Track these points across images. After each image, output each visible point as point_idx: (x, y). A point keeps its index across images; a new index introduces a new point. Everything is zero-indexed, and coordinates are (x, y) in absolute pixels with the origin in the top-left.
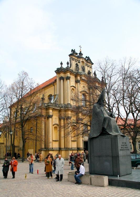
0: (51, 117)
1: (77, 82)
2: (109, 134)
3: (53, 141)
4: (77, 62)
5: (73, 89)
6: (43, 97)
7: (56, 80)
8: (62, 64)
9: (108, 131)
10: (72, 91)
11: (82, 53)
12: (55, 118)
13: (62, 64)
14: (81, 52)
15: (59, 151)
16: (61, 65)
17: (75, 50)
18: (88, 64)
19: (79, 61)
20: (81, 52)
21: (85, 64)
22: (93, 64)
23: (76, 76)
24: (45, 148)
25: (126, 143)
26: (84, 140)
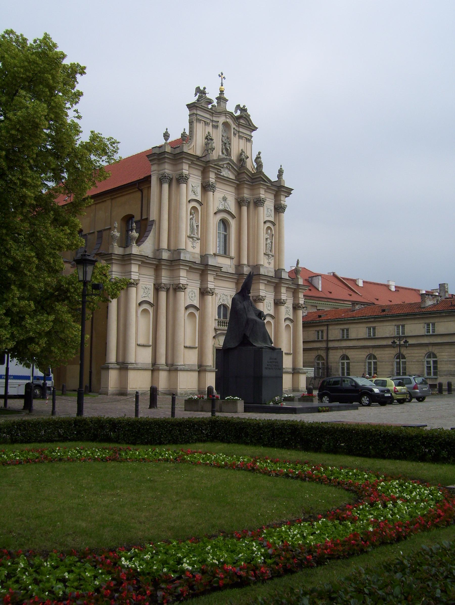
0: (135, 284)
2: (252, 345)
3: (139, 345)
4: (211, 124)
5: (194, 208)
7: (150, 177)
9: (251, 340)
11: (226, 96)
12: (144, 286)
13: (166, 136)
14: (222, 92)
15: (153, 371)
17: (205, 88)
18: (241, 130)
20: (222, 92)
23: (204, 173)
24: (117, 363)
25: (276, 359)
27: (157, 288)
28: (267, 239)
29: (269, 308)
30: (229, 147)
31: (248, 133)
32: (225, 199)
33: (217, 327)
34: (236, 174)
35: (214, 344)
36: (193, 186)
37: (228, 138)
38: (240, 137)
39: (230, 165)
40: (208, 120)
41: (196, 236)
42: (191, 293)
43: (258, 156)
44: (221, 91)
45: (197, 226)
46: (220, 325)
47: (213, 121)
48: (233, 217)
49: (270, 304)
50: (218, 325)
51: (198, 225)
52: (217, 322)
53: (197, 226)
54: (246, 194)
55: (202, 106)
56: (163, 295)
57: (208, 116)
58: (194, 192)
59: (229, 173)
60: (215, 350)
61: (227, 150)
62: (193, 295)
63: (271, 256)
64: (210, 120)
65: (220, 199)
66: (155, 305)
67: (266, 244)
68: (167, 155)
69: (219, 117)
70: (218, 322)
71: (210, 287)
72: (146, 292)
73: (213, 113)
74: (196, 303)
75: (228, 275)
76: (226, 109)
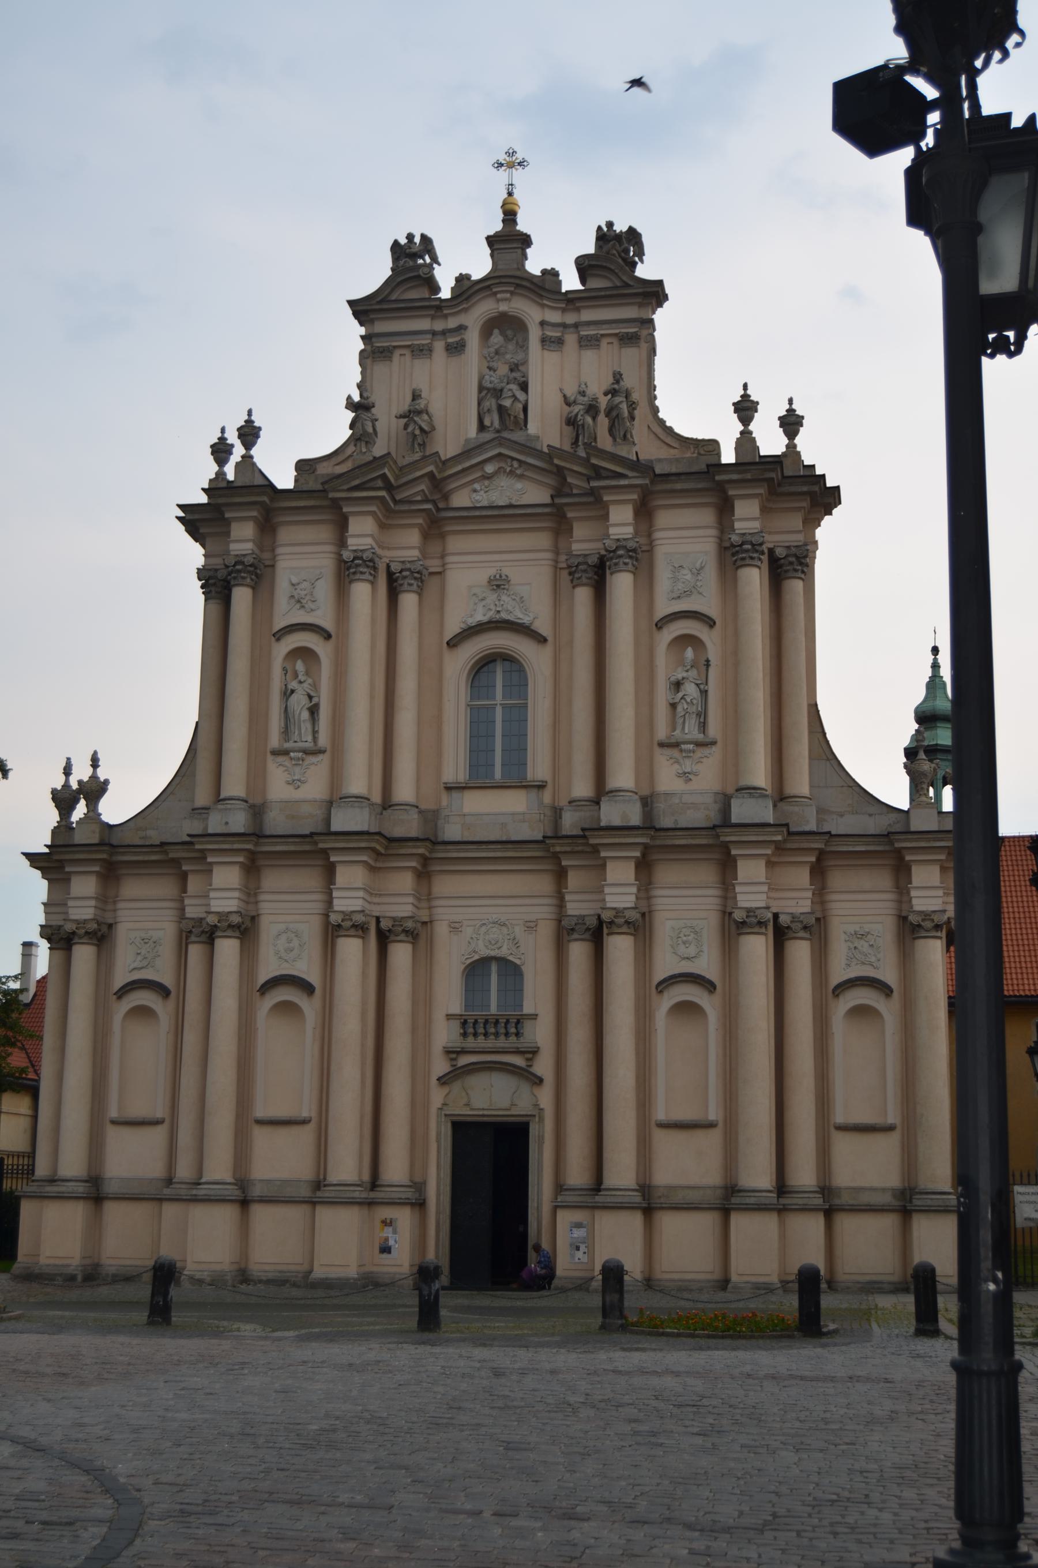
4: (439, 346)
11: (522, 226)
13: (220, 451)
14: (510, 215)
20: (510, 215)
26: (460, 1110)
29: (692, 951)
30: (515, 398)
31: (630, 312)
34: (551, 481)
35: (445, 1104)
36: (295, 580)
37: (514, 368)
38: (589, 343)
39: (513, 459)
40: (424, 336)
41: (309, 745)
42: (284, 937)
43: (616, 386)
45: (314, 711)
46: (475, 1035)
47: (444, 333)
48: (542, 640)
49: (696, 933)
50: (465, 1035)
52: (456, 1025)
53: (314, 711)
55: (396, 301)
56: (195, 952)
57: (424, 324)
58: (299, 601)
59: (519, 485)
60: (447, 1130)
61: (501, 409)
62: (295, 943)
63: (691, 746)
64: (434, 333)
67: (673, 706)
70: (464, 1023)
71: (344, 909)
72: (143, 952)
74: (308, 968)
75: (494, 850)
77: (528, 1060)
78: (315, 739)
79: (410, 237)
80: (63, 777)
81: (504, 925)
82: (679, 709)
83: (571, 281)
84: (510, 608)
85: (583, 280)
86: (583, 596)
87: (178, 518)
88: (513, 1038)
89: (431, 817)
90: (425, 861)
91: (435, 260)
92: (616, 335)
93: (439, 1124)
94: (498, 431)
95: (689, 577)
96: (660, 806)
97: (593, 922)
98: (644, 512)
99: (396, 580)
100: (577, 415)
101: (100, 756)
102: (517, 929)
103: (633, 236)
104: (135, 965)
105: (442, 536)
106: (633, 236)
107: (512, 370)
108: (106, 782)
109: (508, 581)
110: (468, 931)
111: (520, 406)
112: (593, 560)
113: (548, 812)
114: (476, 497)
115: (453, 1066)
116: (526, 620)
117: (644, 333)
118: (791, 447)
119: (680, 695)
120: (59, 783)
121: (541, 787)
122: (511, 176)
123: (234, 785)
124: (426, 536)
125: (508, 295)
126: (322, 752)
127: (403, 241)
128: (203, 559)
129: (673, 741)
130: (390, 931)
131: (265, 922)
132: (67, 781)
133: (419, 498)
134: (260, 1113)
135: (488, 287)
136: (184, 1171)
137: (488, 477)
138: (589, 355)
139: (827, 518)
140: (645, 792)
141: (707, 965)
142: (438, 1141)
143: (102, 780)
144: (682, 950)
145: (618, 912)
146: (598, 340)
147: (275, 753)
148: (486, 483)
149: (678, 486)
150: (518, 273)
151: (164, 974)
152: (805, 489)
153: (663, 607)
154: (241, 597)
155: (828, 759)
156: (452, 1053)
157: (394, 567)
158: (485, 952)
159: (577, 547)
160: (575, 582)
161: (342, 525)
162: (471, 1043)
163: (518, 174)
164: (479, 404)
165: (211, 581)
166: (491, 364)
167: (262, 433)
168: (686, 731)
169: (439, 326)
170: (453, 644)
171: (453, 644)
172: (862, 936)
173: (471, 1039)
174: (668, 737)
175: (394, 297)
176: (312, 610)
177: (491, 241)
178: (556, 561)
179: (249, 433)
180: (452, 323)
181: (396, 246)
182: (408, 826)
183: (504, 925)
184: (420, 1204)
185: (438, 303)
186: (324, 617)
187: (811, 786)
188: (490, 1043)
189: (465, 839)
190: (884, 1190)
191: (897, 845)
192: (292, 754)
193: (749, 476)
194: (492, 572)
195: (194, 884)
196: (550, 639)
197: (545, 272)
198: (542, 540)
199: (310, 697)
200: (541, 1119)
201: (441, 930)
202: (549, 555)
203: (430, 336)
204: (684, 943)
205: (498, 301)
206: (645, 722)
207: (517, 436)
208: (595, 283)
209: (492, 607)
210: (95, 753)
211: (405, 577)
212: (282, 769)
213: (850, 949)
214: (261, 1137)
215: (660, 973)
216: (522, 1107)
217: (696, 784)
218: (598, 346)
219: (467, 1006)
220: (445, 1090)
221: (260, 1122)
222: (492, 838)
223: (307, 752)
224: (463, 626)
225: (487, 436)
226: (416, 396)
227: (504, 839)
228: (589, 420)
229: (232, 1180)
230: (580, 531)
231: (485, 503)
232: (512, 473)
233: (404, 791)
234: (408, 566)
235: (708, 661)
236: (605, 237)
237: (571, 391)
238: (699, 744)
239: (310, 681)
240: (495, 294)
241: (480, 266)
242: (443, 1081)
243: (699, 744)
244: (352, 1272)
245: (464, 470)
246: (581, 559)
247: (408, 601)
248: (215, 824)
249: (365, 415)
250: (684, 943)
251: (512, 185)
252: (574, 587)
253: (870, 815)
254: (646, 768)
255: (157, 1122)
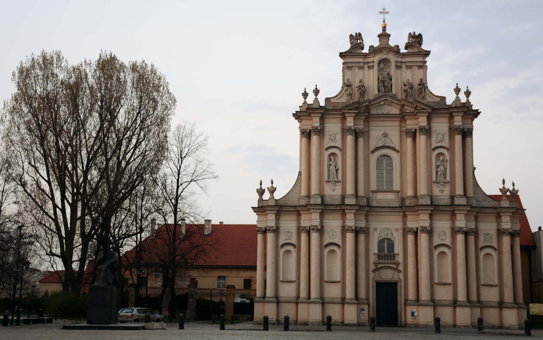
1: (345, 131)
6: (261, 188)
8: (305, 95)
10: (330, 160)
11: (388, 31)
13: (305, 95)
14: (384, 28)
16: (305, 98)
19: (371, 64)
20: (384, 28)
21: (393, 65)
22: (427, 53)
26: (379, 280)
27: (300, 230)
28: (438, 167)
29: (444, 238)
30: (388, 83)
31: (420, 59)
32: (385, 135)
33: (377, 261)
34: (399, 107)
35: (374, 277)
36: (330, 134)
38: (408, 67)
39: (389, 100)
41: (336, 180)
42: (331, 232)
44: (383, 28)
45: (337, 170)
46: (382, 259)
48: (398, 151)
49: (445, 233)
50: (379, 259)
51: (338, 169)
52: (376, 257)
54: (411, 124)
55: (353, 53)
56: (304, 236)
57: (361, 60)
58: (332, 140)
59: (390, 108)
60: (375, 284)
63: (443, 183)
64: (364, 63)
65: (378, 137)
66: (297, 246)
67: (437, 172)
68: (300, 113)
69: (374, 57)
70: (379, 256)
72: (288, 235)
73: (366, 56)
74: (338, 240)
75: (387, 209)
76: (388, 44)
77: (397, 266)
78: (337, 178)
79: (356, 34)
80: (260, 186)
81: (389, 229)
82: (439, 173)
83: (403, 50)
84: (388, 142)
85: (406, 48)
86: (409, 140)
87: (293, 114)
88: (392, 260)
89: (368, 199)
90: (368, 211)
91: (362, 40)
92: (417, 65)
93: (372, 282)
94: (384, 93)
95: (441, 137)
96: (434, 199)
97: (415, 230)
98: (429, 119)
99: (357, 134)
100: (407, 89)
101: (273, 180)
102: (393, 230)
103: (420, 36)
104: (286, 238)
105: (368, 121)
106: (420, 36)
107: (387, 75)
108: (276, 188)
109: (388, 135)
110: (379, 231)
111: (390, 85)
112: (413, 130)
113: (400, 199)
114: (378, 111)
115: (376, 267)
116: (393, 146)
117: (424, 65)
118: (468, 100)
119: (439, 169)
120: (259, 187)
121: (398, 192)
122: (384, 16)
123: (314, 191)
124: (364, 121)
125: (386, 53)
126: (340, 182)
127: (354, 35)
128: (299, 124)
129: (438, 181)
130: (359, 231)
131: (325, 228)
132: (261, 187)
133: (363, 111)
134: (326, 279)
135: (381, 51)
136: (303, 294)
137: (382, 105)
138: (409, 71)
139: (475, 119)
140: (430, 195)
141: (448, 242)
142: (372, 287)
143: (274, 187)
144: (441, 237)
145: (426, 227)
146: (412, 67)
147: (327, 182)
148: (381, 107)
149: (439, 112)
150: (387, 46)
151: (294, 241)
152: (473, 113)
153: (434, 145)
154: (315, 139)
155: (477, 186)
156: (375, 264)
157: (357, 131)
158: (384, 237)
159: (408, 127)
160: (408, 136)
161: (344, 118)
162: (381, 261)
163: (386, 16)
164: (378, 84)
165: (305, 133)
166: (381, 73)
167: (320, 92)
168: (441, 179)
169: (366, 60)
170: (372, 152)
171: (372, 152)
172: (488, 234)
173: (380, 260)
174: (436, 180)
175: (352, 52)
176: (336, 142)
177: (379, 36)
178: (401, 130)
179: (316, 92)
180: (370, 60)
181: (351, 36)
182: (364, 202)
183: (389, 229)
184: (369, 305)
185: (366, 54)
186: (339, 144)
187: (474, 194)
188: (386, 261)
189: (378, 206)
190: (495, 302)
191: (499, 211)
192: (332, 182)
193: (460, 110)
194: (383, 132)
195: (303, 217)
196: (400, 151)
197: (395, 46)
198: (397, 123)
199: (335, 166)
200: (401, 282)
201: (371, 230)
202: (398, 128)
203: (363, 63)
204: (442, 236)
205: (384, 54)
206: (429, 176)
207: (390, 94)
208: (411, 50)
209: (383, 142)
210: (272, 180)
211: (360, 134)
212: (329, 186)
213: (484, 238)
214: (327, 287)
215: (435, 244)
216: (396, 278)
217: (443, 194)
218: (412, 69)
219: (379, 251)
220: (374, 274)
221: (326, 282)
222: (385, 206)
223: (336, 182)
224: (375, 147)
225: (381, 94)
226: (361, 81)
227: (389, 206)
228: (410, 90)
229: (319, 297)
230: (409, 122)
231: (380, 113)
232: (388, 104)
233: (361, 193)
234: (361, 130)
235: (447, 160)
236: (412, 36)
237: (405, 83)
238: (445, 183)
239: (335, 162)
240: (383, 52)
241: (376, 43)
242: (373, 271)
243: (445, 183)
244: (356, 322)
245: (375, 103)
246: (410, 130)
247: (361, 141)
248: (312, 201)
249: (350, 88)
250: (442, 236)
251: (384, 19)
252: (407, 138)
253: (489, 202)
254: (430, 188)
255: (294, 282)
